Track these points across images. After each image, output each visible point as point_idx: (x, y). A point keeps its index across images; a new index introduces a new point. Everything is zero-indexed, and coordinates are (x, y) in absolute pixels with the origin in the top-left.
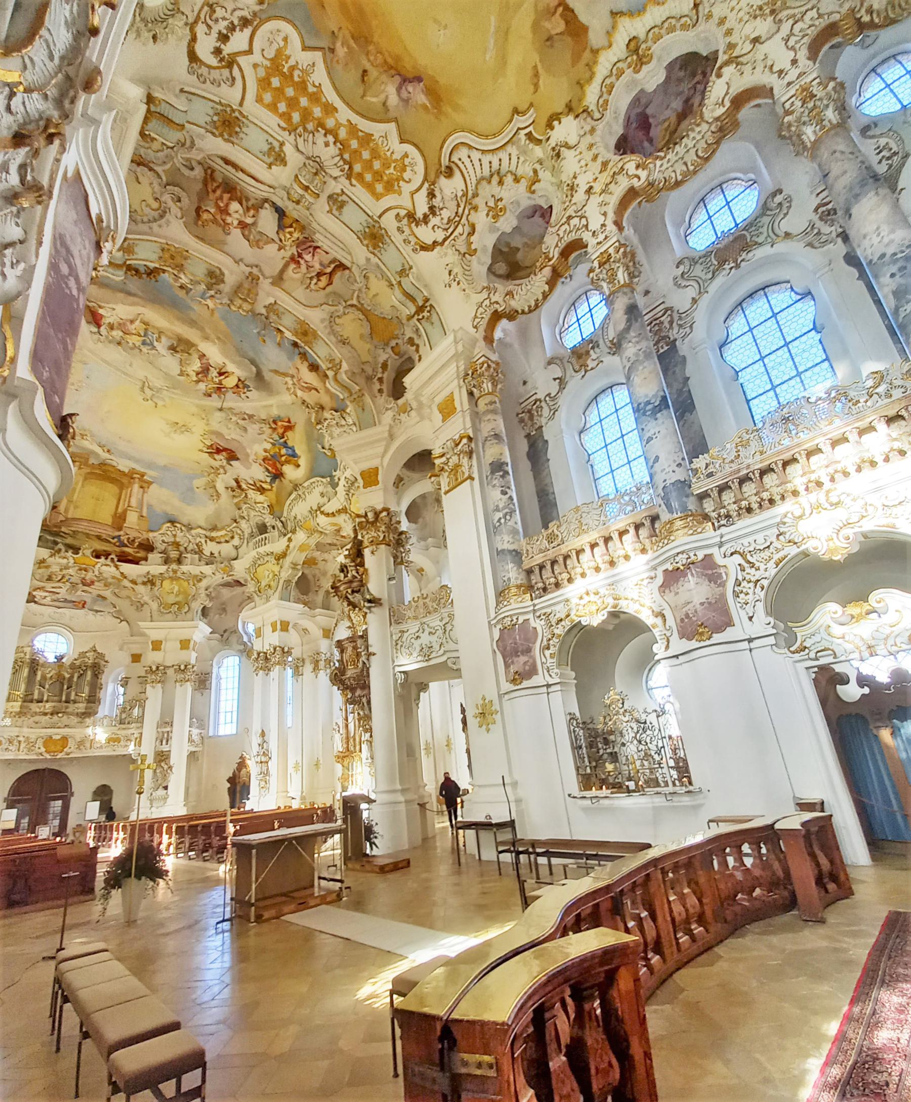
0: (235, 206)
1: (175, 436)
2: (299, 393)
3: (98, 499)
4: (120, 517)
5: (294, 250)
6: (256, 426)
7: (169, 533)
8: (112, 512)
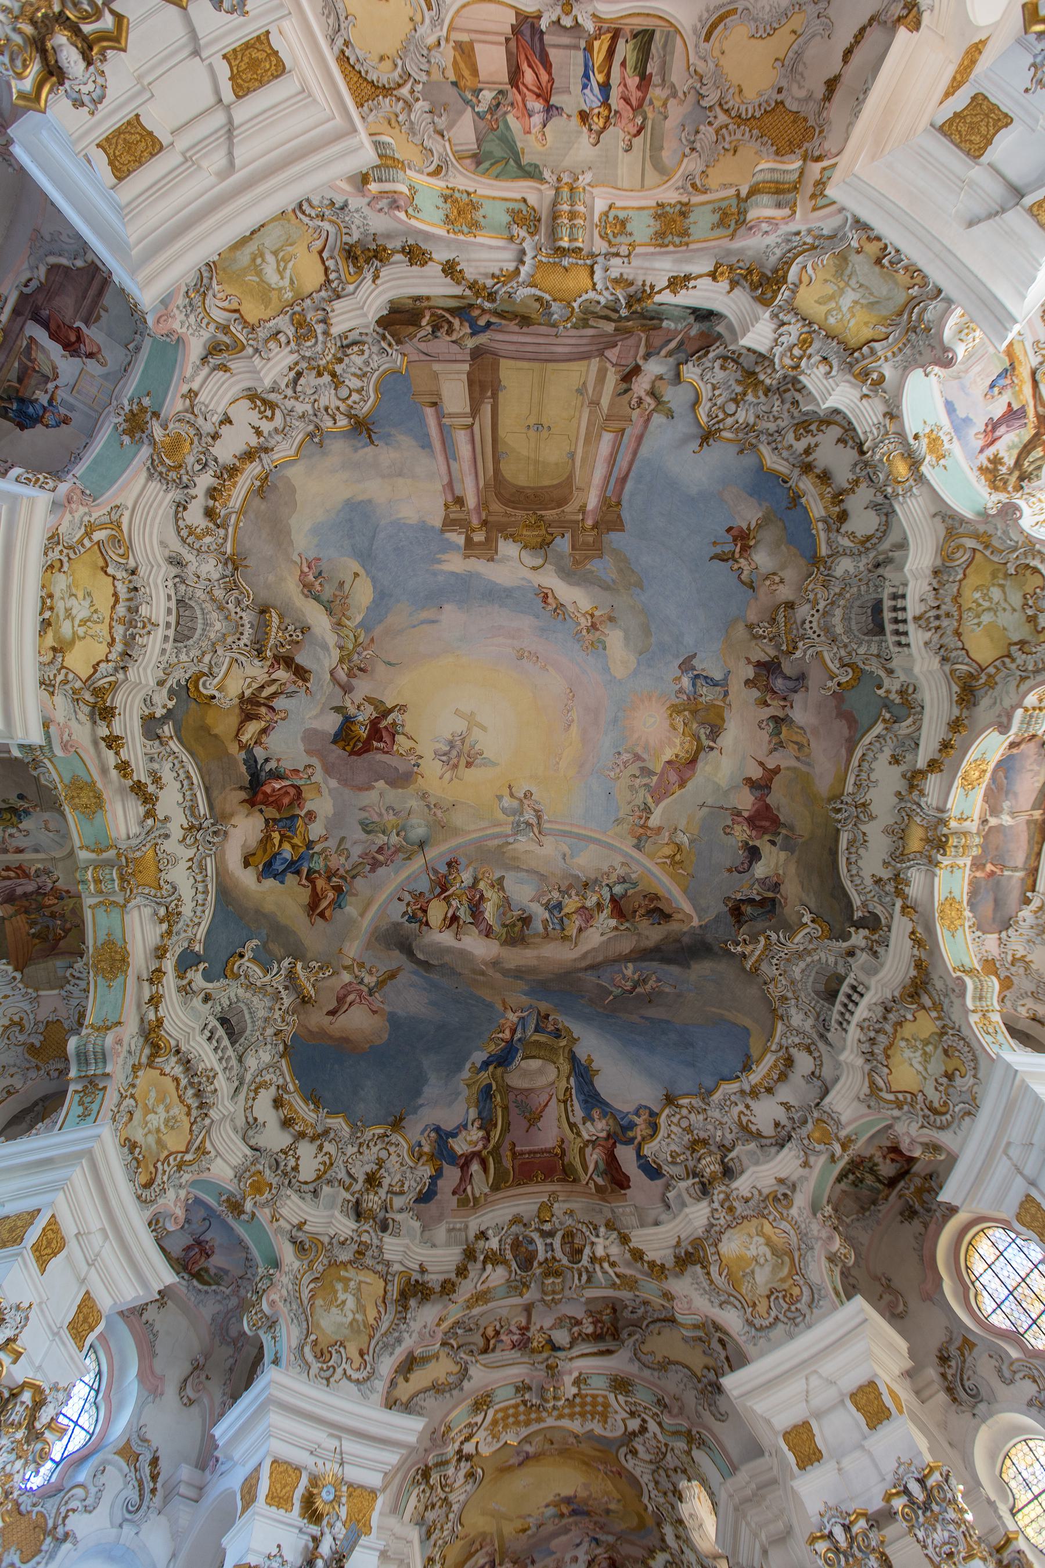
0: (590, 1330)
1: (460, 726)
2: (346, 977)
3: (539, 426)
4: (483, 388)
5: (530, 1334)
6: (356, 851)
7: (354, 383)
8: (501, 395)
